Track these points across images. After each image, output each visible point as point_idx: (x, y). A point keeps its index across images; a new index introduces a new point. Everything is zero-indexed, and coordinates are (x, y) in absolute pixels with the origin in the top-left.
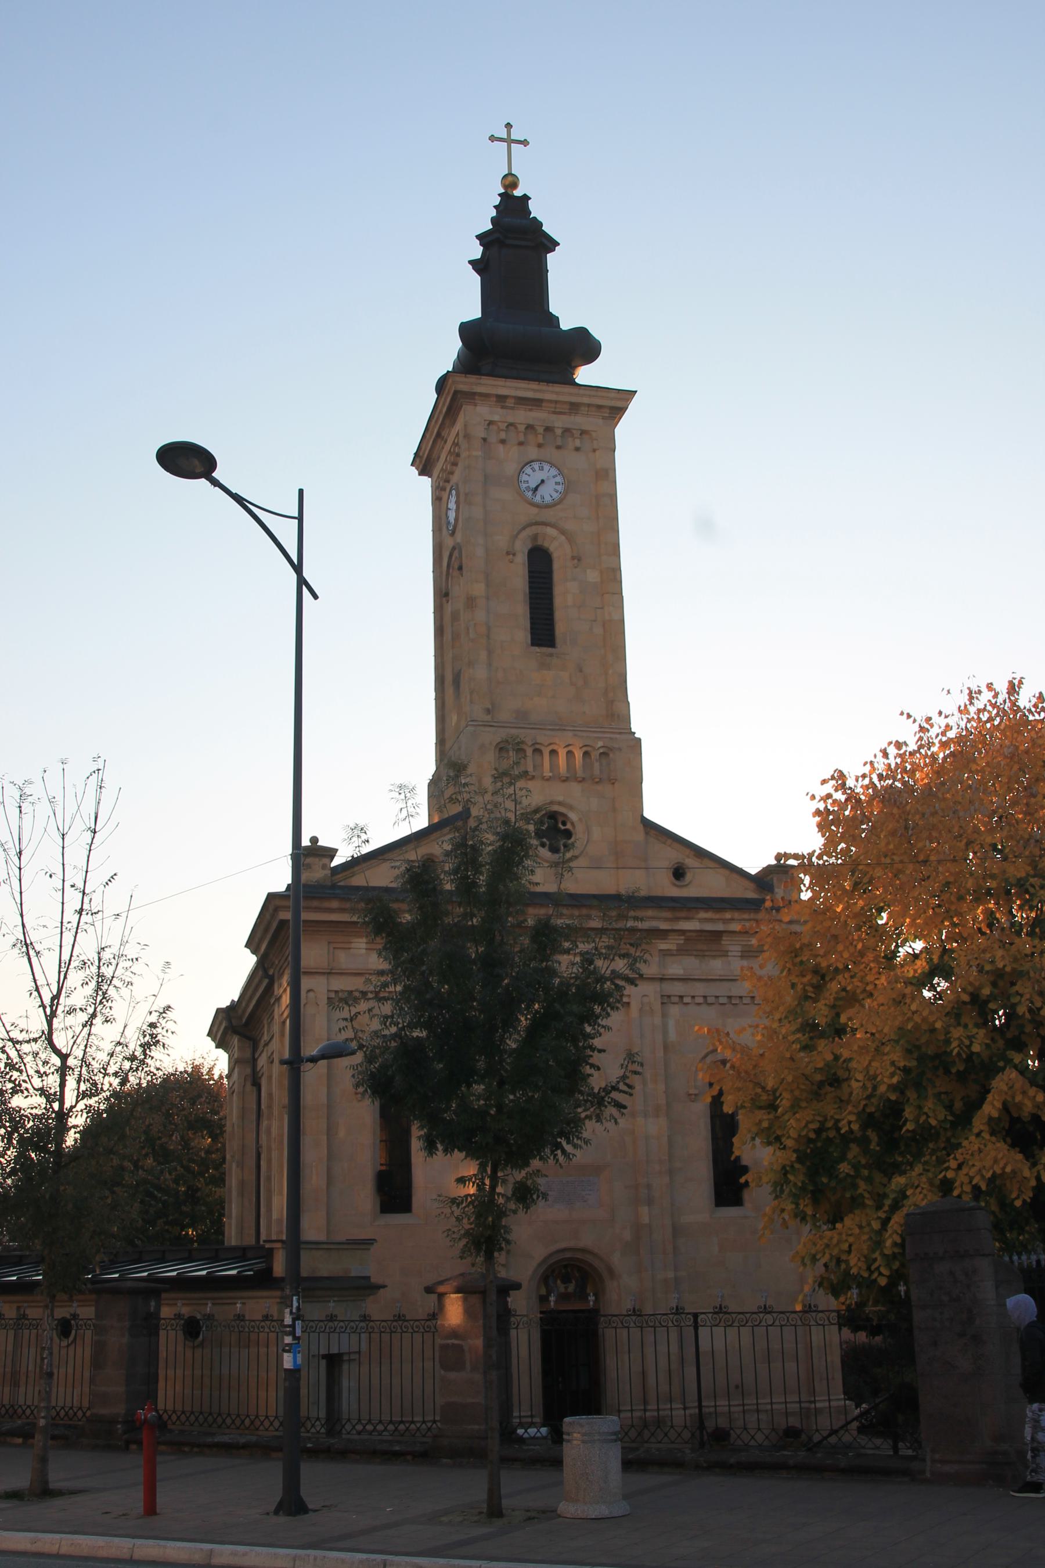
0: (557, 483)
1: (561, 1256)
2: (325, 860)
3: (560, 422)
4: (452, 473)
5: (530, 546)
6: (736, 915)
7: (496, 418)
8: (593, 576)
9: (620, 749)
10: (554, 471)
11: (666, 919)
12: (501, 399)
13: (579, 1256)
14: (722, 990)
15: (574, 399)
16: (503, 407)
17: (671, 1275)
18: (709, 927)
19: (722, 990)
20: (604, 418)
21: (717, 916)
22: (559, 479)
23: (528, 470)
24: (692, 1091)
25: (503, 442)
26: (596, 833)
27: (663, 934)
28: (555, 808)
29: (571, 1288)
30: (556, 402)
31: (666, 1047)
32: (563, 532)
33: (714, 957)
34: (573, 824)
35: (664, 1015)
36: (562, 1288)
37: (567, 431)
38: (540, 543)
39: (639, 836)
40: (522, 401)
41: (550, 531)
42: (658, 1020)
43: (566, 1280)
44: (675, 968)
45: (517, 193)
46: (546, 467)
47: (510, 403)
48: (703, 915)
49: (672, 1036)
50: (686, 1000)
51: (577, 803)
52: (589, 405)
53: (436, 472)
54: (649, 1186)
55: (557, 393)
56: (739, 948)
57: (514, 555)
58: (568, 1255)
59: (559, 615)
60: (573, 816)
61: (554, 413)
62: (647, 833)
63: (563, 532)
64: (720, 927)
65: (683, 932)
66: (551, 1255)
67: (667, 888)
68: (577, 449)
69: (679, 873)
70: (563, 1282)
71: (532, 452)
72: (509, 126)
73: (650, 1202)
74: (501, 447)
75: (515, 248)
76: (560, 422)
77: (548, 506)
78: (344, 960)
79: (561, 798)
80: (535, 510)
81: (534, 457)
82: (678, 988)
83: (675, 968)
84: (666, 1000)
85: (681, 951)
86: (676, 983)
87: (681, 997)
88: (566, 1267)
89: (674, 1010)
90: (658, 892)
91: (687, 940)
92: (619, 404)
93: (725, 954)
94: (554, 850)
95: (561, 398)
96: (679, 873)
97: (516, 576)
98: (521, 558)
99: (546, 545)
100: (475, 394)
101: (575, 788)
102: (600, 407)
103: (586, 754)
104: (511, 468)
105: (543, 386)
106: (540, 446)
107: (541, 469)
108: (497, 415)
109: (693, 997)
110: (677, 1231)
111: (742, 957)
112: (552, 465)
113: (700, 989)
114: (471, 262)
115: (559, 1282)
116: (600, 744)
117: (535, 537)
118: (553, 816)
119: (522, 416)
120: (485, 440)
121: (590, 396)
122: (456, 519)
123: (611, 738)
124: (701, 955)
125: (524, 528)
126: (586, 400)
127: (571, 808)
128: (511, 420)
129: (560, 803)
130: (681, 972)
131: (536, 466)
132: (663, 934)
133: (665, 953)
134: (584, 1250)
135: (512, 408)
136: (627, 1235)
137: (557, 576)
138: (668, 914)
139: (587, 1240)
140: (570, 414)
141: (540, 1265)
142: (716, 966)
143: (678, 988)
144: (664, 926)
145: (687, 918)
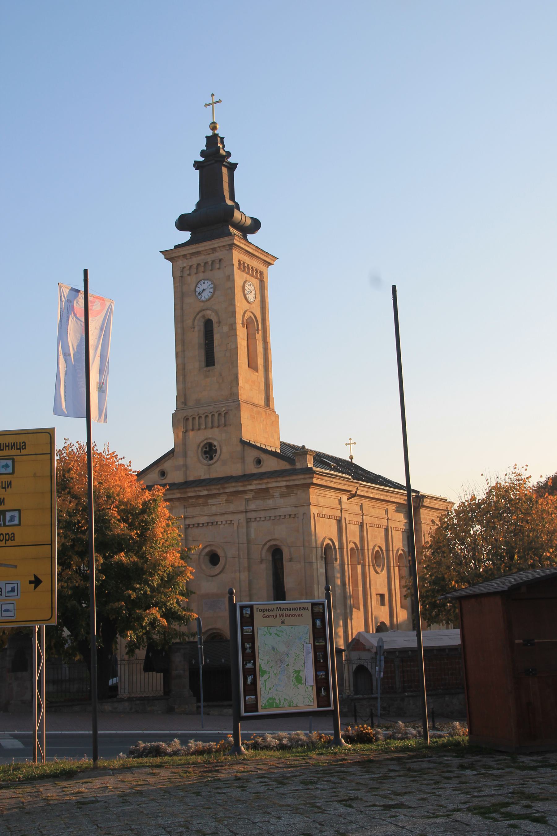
0: (210, 288)
5: (203, 320)
6: (269, 480)
7: (185, 265)
8: (225, 329)
9: (232, 410)
10: (209, 283)
11: (241, 486)
12: (184, 256)
14: (272, 513)
15: (212, 247)
16: (187, 259)
18: (259, 487)
19: (272, 513)
20: (228, 250)
21: (261, 482)
23: (199, 285)
25: (189, 275)
26: (224, 450)
27: (245, 492)
30: (206, 250)
31: (249, 542)
33: (269, 499)
35: (248, 527)
37: (213, 262)
38: (207, 318)
39: (239, 448)
40: (192, 254)
41: (209, 312)
42: (244, 530)
44: (252, 506)
45: (216, 132)
46: (206, 282)
47: (188, 256)
49: (253, 536)
50: (258, 519)
52: (219, 247)
55: (204, 246)
56: (278, 494)
57: (194, 328)
58: (215, 631)
60: (215, 443)
61: (207, 254)
62: (244, 446)
64: (264, 486)
65: (252, 490)
67: (252, 469)
68: (219, 269)
69: (259, 462)
74: (189, 277)
75: (214, 165)
76: (209, 258)
79: (210, 436)
80: (202, 304)
81: (201, 278)
82: (252, 515)
83: (252, 506)
84: (248, 521)
85: (254, 498)
86: (253, 513)
87: (255, 518)
90: (248, 472)
91: (255, 493)
92: (231, 242)
93: (273, 497)
95: (206, 248)
96: (259, 462)
97: (196, 337)
99: (210, 318)
100: (173, 258)
101: (216, 430)
102: (224, 246)
103: (219, 414)
105: (197, 245)
106: (204, 272)
107: (204, 283)
109: (260, 518)
111: (281, 497)
112: (208, 280)
113: (262, 514)
116: (224, 409)
117: (204, 316)
119: (195, 261)
120: (182, 277)
121: (218, 243)
123: (228, 406)
125: (198, 314)
127: (214, 439)
128: (190, 264)
129: (210, 439)
130: (255, 507)
131: (202, 282)
132: (245, 492)
133: (247, 500)
135: (190, 258)
138: (240, 484)
140: (213, 253)
142: (270, 503)
144: (241, 489)
145: (251, 484)
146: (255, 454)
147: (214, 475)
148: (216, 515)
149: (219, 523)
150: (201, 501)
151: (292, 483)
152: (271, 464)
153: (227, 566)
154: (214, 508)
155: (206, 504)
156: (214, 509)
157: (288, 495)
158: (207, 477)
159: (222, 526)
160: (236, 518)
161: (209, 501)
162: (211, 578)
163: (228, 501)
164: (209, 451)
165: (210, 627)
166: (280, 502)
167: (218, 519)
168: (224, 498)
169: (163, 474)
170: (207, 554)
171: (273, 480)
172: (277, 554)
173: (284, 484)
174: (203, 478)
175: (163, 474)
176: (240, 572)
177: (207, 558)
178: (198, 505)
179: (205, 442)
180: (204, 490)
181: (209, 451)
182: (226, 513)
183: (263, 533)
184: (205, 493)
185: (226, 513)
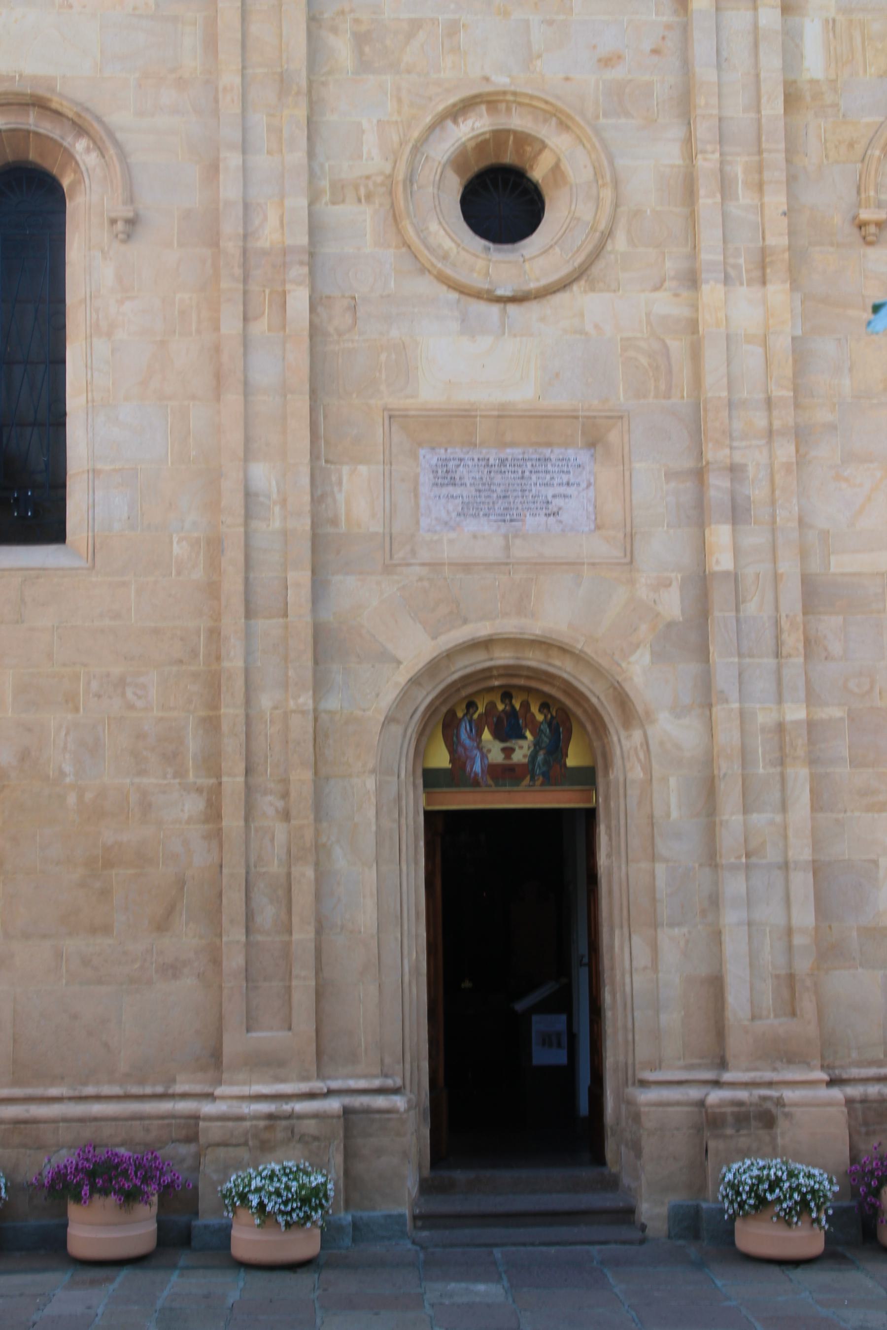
1: (478, 661)
13: (533, 659)
17: (795, 713)
24: (865, 215)
29: (522, 751)
31: (792, 98)
36: (495, 752)
43: (508, 728)
49: (814, 64)
54: (735, 470)
58: (503, 657)
66: (450, 655)
70: (500, 735)
73: (738, 514)
88: (507, 695)
110: (815, 594)
115: (487, 735)
134: (543, 644)
136: (672, 605)
139: (555, 614)
141: (415, 681)
153: (620, 243)
162: (495, 309)
165: (483, 629)
170: (459, 162)
176: (727, 280)
177: (455, 187)
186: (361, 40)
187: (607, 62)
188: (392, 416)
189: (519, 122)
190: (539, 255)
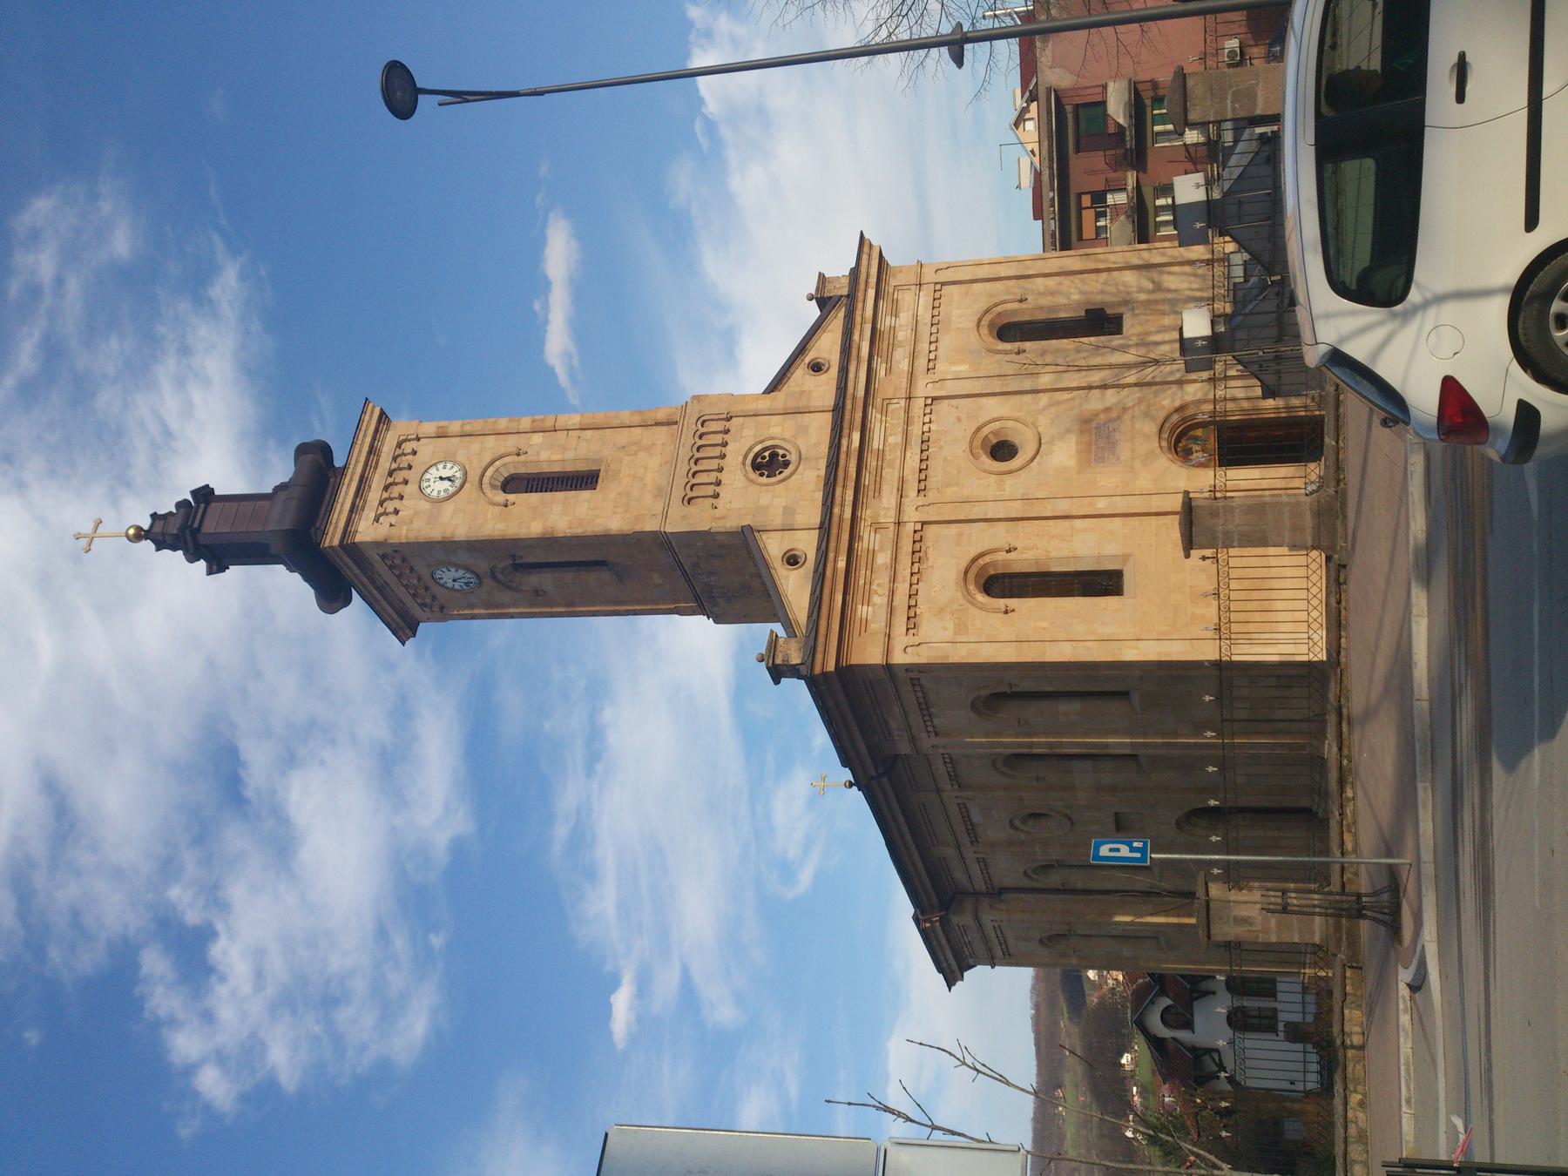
2: (781, 641)
3: (385, 463)
4: (419, 579)
10: (433, 470)
14: (925, 330)
19: (925, 330)
22: (440, 466)
25: (396, 512)
28: (749, 461)
30: (366, 464)
32: (491, 463)
34: (765, 449)
46: (427, 476)
48: (856, 337)
50: (932, 356)
51: (744, 441)
52: (374, 439)
53: (417, 611)
59: (569, 468)
63: (491, 463)
69: (817, 368)
71: (411, 488)
72: (78, 537)
77: (466, 474)
78: (878, 625)
80: (467, 485)
81: (416, 487)
82: (921, 363)
83: (904, 365)
85: (889, 360)
89: (941, 367)
93: (893, 329)
94: (786, 464)
96: (817, 368)
98: (511, 497)
102: (376, 431)
104: (424, 505)
106: (406, 482)
108: (369, 514)
113: (924, 346)
114: (210, 572)
117: (493, 486)
118: (756, 467)
119: (374, 494)
122: (467, 569)
124: (892, 346)
126: (368, 440)
127: (750, 449)
129: (745, 457)
131: (425, 484)
133: (889, 371)
137: (533, 470)
143: (921, 363)
146: (800, 375)
147: (824, 449)
148: (906, 434)
149: (926, 428)
150: (871, 462)
151: (873, 280)
152: (828, 346)
154: (891, 440)
155: (881, 454)
156: (895, 439)
157: (895, 302)
158: (823, 464)
159: (933, 427)
160: (923, 389)
161: (875, 446)
163: (884, 411)
164: (769, 463)
166: (905, 318)
167: (916, 430)
168: (875, 415)
169: (792, 560)
171: (860, 305)
172: (1010, 331)
173: (871, 293)
174: (823, 472)
175: (792, 560)
178: (879, 471)
179: (749, 468)
180: (849, 436)
181: (769, 463)
182: (907, 411)
183: (962, 355)
184: (856, 436)
185: (907, 411)
186: (948, 485)
187: (959, 420)
188: (1079, 472)
189: (978, 443)
190: (1025, 441)
